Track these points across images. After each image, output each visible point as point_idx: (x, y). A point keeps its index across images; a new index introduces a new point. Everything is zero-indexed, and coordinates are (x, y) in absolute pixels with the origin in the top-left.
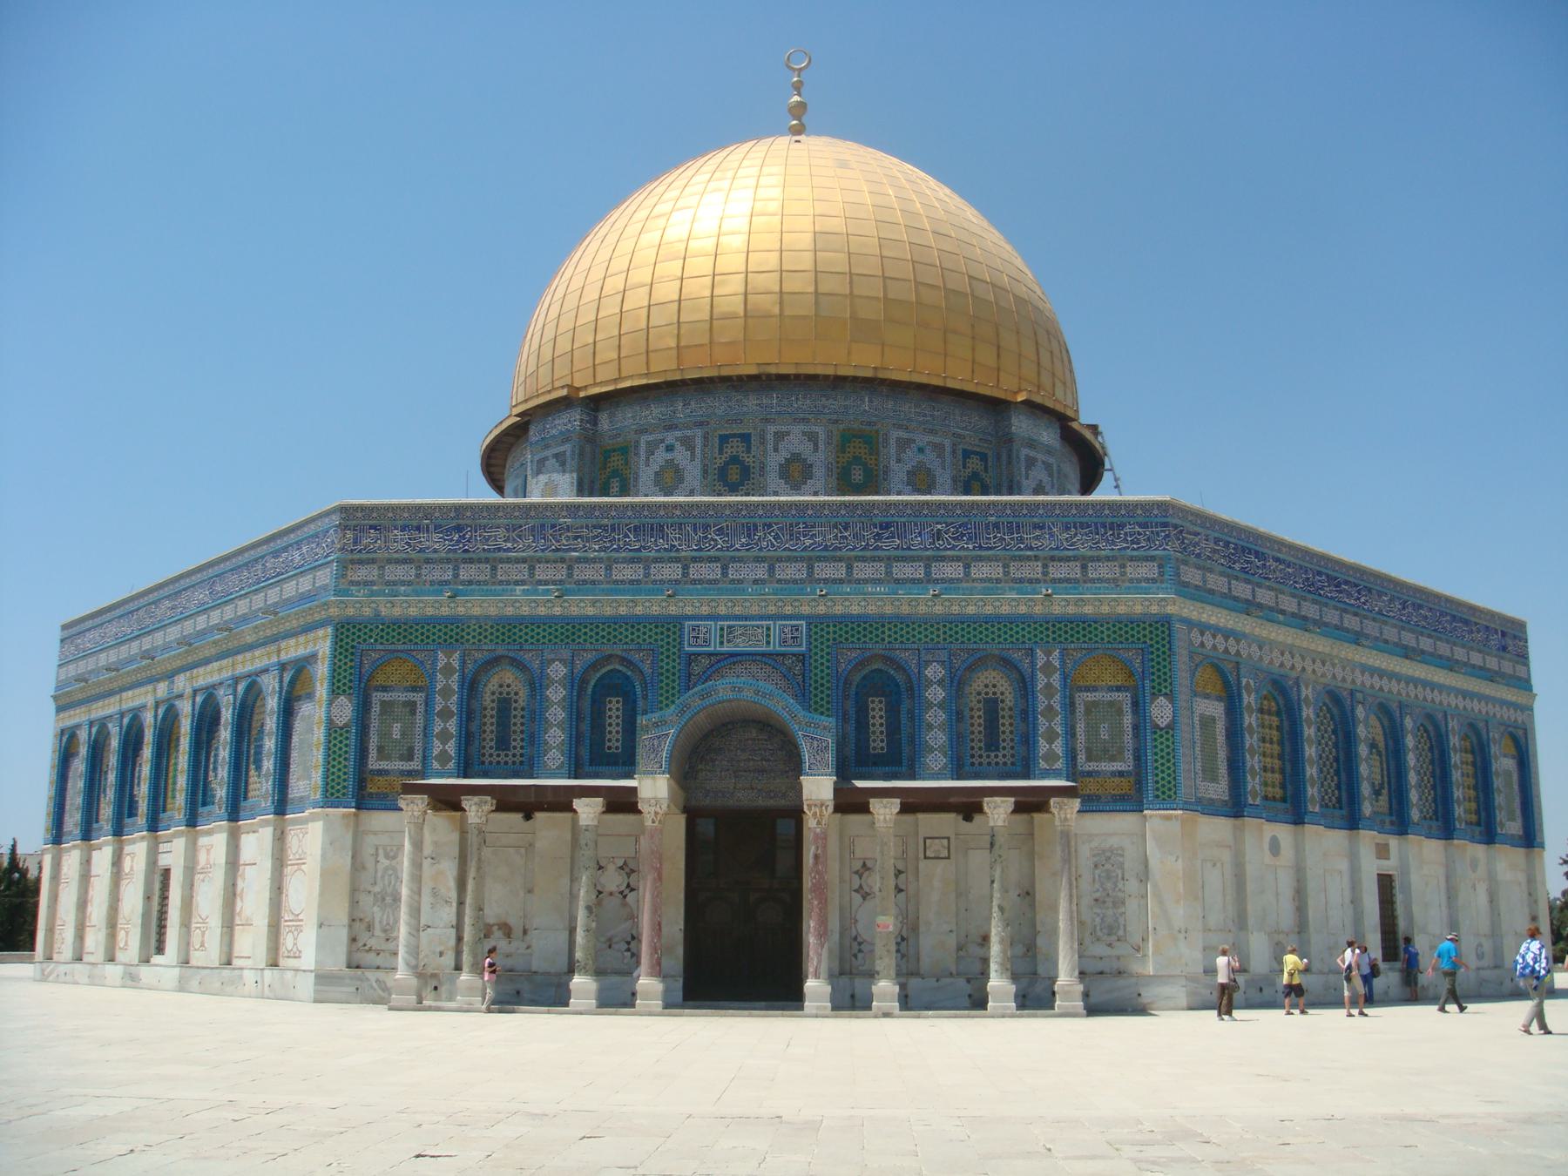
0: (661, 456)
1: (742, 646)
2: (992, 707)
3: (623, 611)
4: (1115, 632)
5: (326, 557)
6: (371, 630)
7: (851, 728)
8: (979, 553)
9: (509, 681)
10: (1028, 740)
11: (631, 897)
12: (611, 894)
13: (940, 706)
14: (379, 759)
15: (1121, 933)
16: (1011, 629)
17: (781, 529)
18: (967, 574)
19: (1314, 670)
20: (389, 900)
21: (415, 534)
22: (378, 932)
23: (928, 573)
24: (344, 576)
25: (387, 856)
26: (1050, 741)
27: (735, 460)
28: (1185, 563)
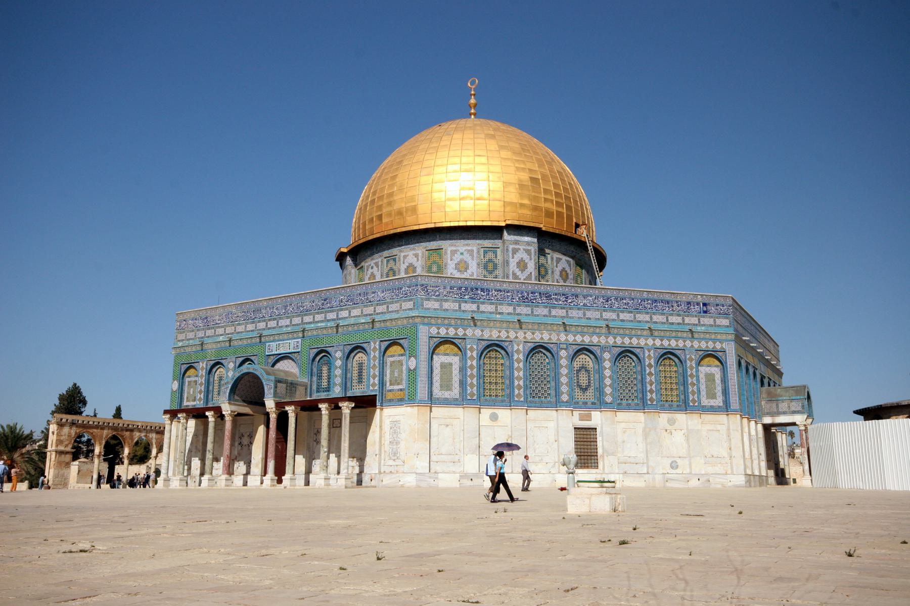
0: (370, 271)
2: (361, 365)
4: (397, 332)
7: (315, 379)
8: (355, 306)
12: (245, 446)
13: (340, 368)
14: (187, 402)
15: (398, 455)
16: (363, 335)
18: (350, 315)
19: (525, 338)
21: (195, 321)
26: (374, 379)
27: (391, 269)
28: (428, 299)
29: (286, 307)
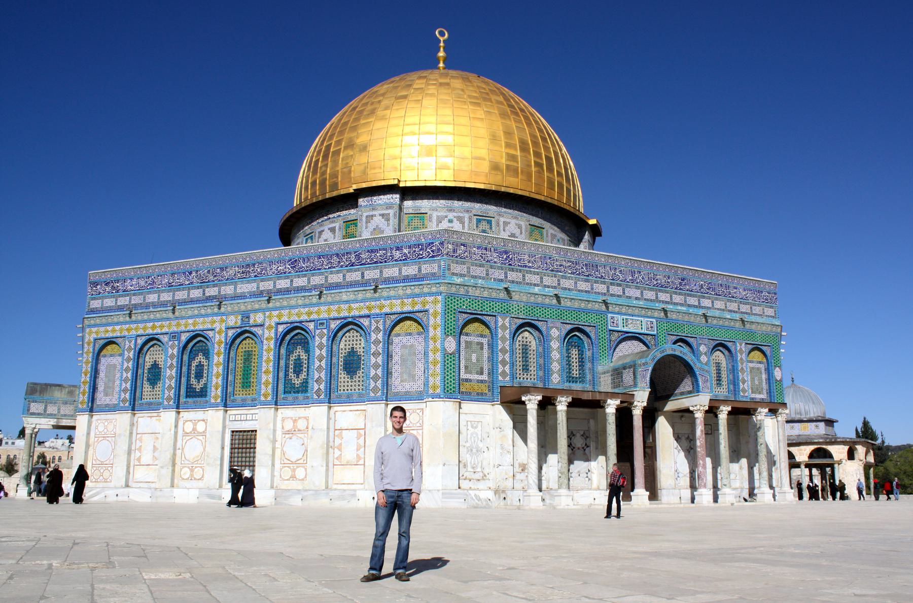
1: (631, 328)
3: (583, 305)
5: (433, 256)
6: (464, 301)
9: (527, 336)
10: (734, 382)
11: (587, 450)
12: (579, 448)
14: (466, 373)
17: (644, 274)
18: (713, 305)
20: (474, 450)
22: (470, 469)
23: (699, 303)
24: (449, 269)
25: (472, 427)
29: (633, 273)
